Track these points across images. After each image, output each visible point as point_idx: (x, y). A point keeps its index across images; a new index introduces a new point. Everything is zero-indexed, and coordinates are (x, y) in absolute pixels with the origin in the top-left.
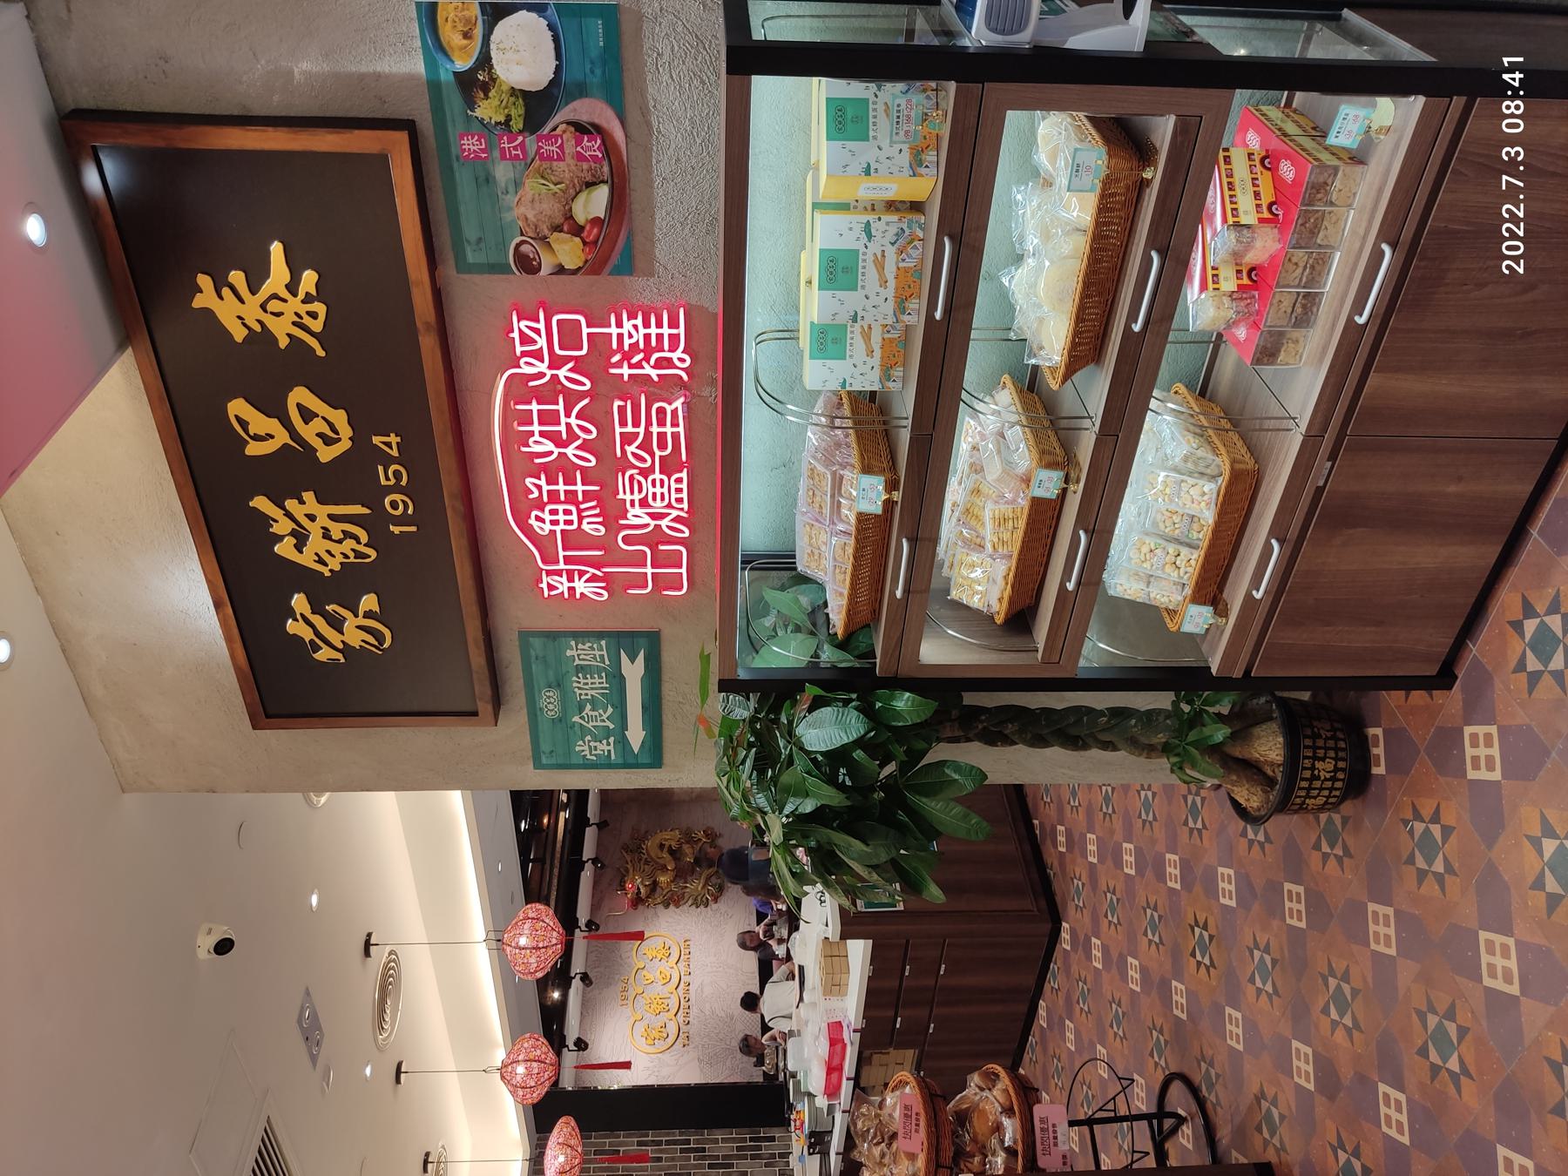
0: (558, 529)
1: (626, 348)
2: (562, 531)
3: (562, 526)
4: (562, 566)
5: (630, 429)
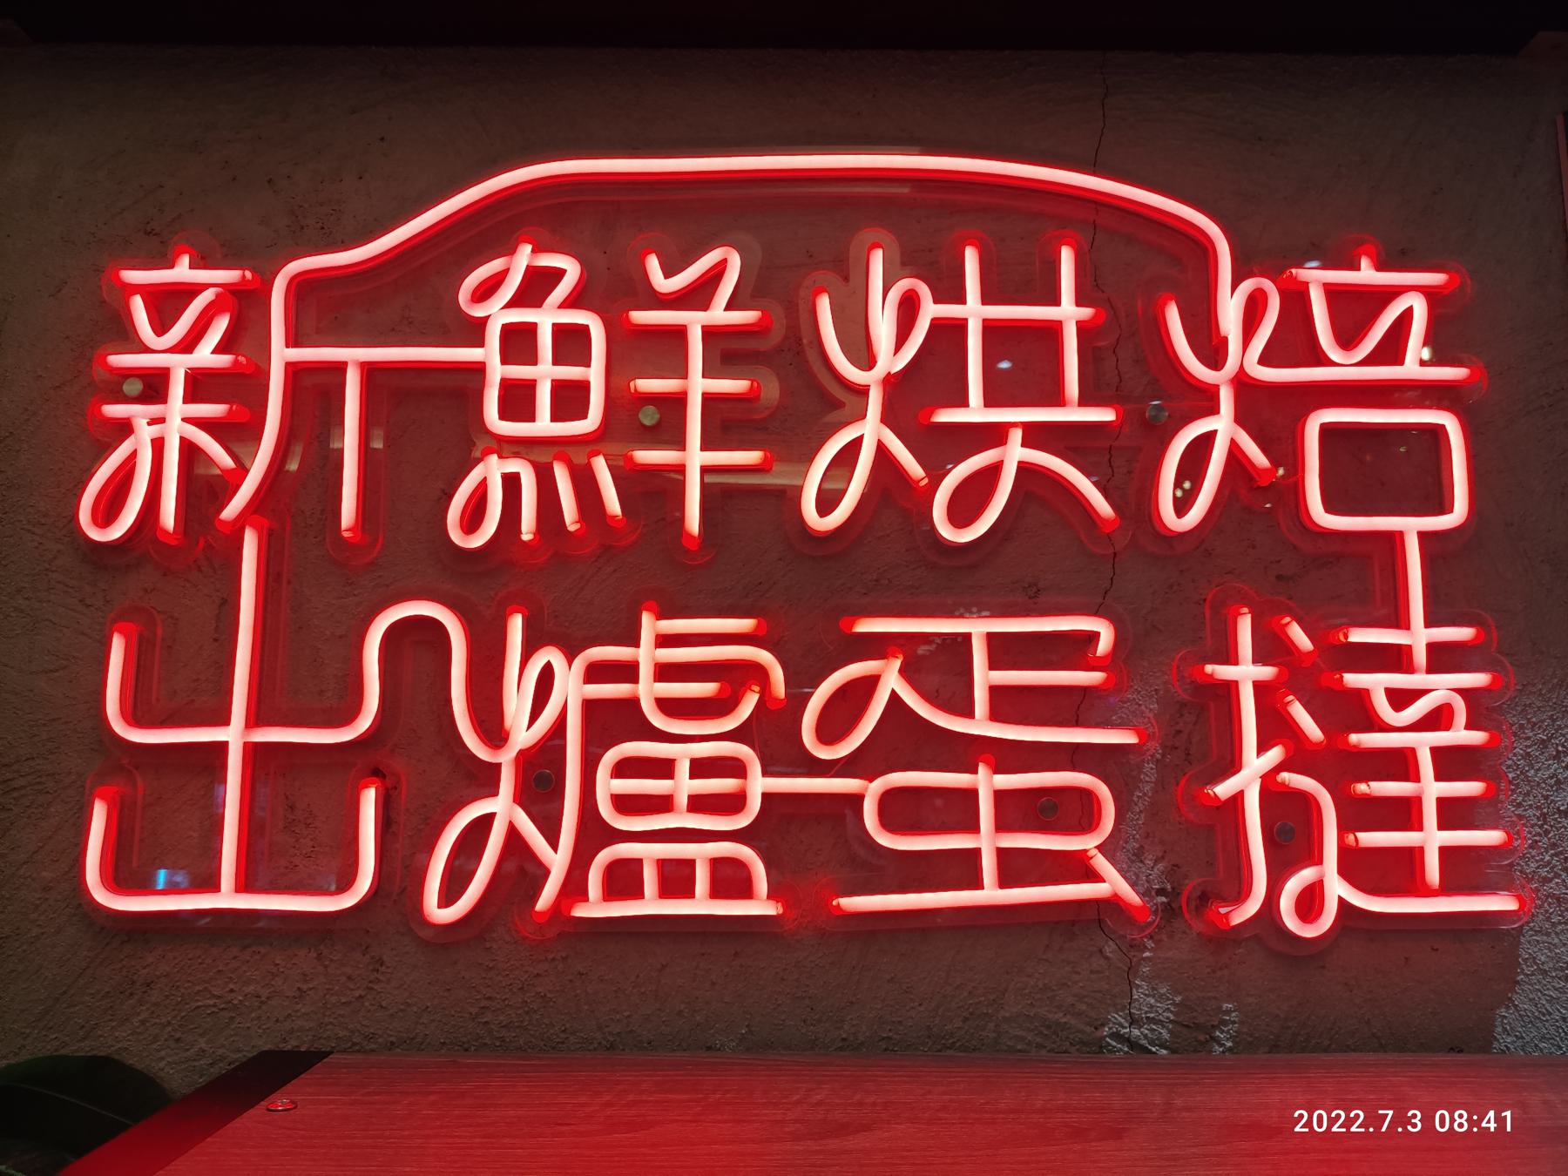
0: (490, 353)
1: (1353, 679)
2: (479, 369)
3: (497, 370)
4: (281, 353)
5: (983, 677)
